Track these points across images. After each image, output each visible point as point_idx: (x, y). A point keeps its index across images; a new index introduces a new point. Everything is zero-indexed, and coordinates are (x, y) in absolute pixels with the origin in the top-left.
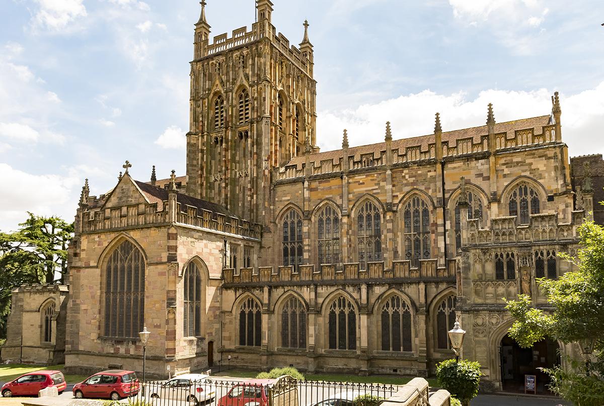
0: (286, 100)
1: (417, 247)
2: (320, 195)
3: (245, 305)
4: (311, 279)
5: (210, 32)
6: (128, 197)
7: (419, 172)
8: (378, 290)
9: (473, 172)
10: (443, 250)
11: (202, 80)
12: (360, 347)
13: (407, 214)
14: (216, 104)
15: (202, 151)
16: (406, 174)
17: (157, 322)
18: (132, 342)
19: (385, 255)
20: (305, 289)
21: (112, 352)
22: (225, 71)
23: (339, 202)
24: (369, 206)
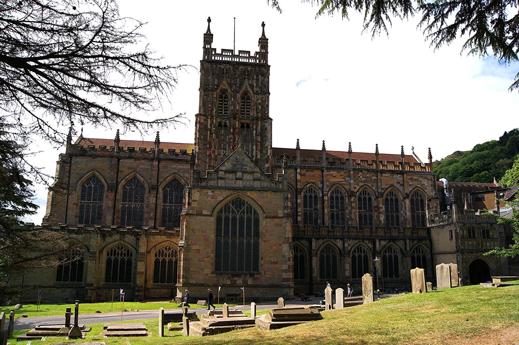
4: (341, 234)
7: (368, 175)
9: (395, 181)
14: (221, 97)
16: (360, 175)
17: (273, 259)
20: (339, 241)
21: (229, 283)
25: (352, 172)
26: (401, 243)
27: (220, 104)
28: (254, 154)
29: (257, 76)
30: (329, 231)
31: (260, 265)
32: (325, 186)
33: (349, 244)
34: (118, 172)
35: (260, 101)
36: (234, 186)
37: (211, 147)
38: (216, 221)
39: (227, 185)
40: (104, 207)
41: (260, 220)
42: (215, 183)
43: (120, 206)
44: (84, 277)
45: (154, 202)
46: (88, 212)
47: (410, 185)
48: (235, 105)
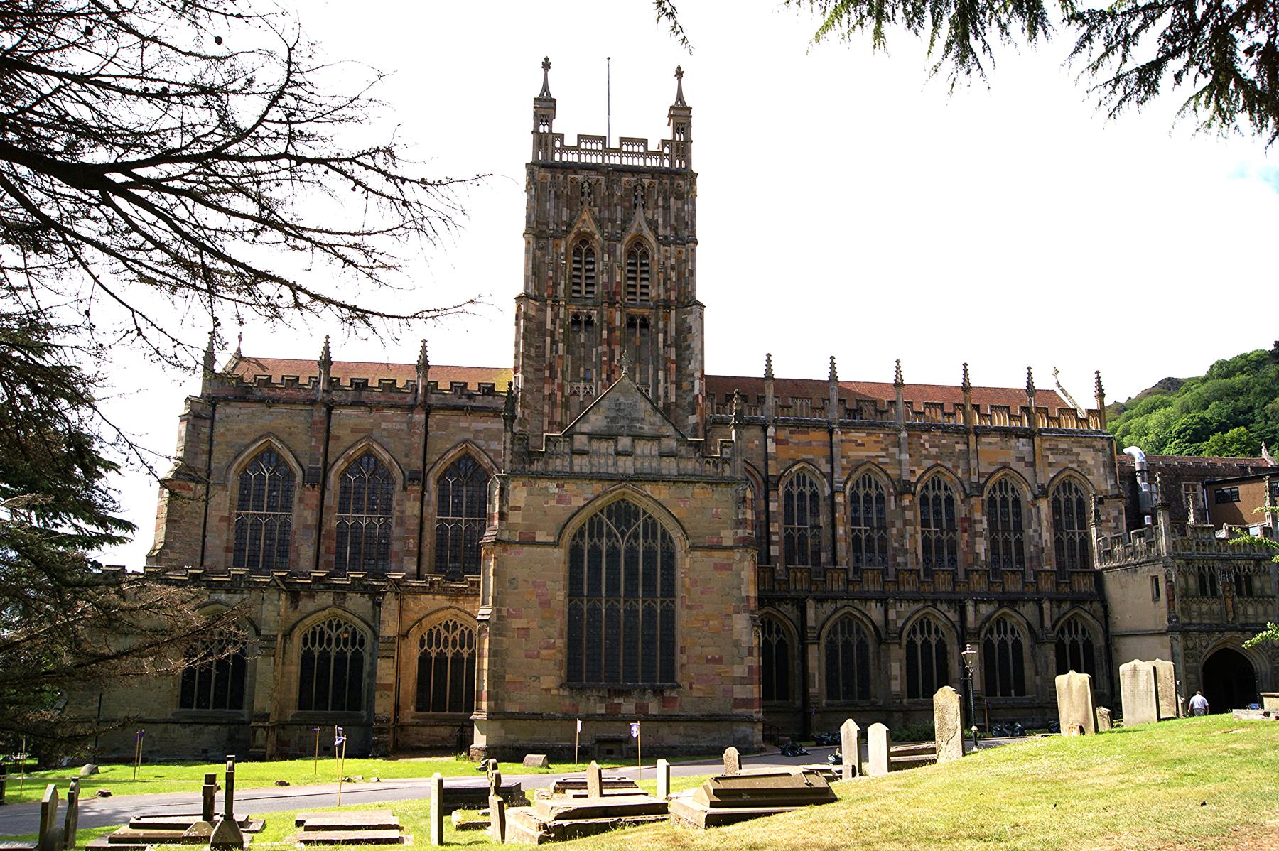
2: (792, 452)
7: (944, 441)
9: (1013, 453)
14: (577, 251)
16: (925, 441)
17: (711, 652)
18: (655, 691)
20: (873, 605)
21: (603, 711)
25: (904, 434)
26: (1029, 610)
27: (575, 269)
28: (661, 392)
30: (849, 582)
31: (678, 665)
32: (838, 470)
33: (901, 613)
34: (328, 439)
35: (673, 261)
36: (612, 470)
37: (553, 376)
38: (568, 559)
39: (594, 470)
40: (293, 527)
41: (678, 555)
42: (566, 463)
43: (332, 523)
44: (246, 698)
45: (417, 512)
46: (255, 538)
47: (1050, 464)
48: (612, 271)
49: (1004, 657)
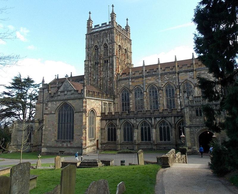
0: (121, 48)
1: (171, 103)
3: (110, 126)
5: (92, 23)
6: (67, 87)
7: (170, 76)
8: (158, 119)
10: (180, 104)
11: (90, 41)
12: (152, 140)
13: (167, 90)
14: (96, 50)
15: (91, 67)
19: (159, 106)
22: (99, 38)
23: (142, 86)
24: (153, 88)
25: (160, 76)
29: (110, 35)
49: (165, 131)
